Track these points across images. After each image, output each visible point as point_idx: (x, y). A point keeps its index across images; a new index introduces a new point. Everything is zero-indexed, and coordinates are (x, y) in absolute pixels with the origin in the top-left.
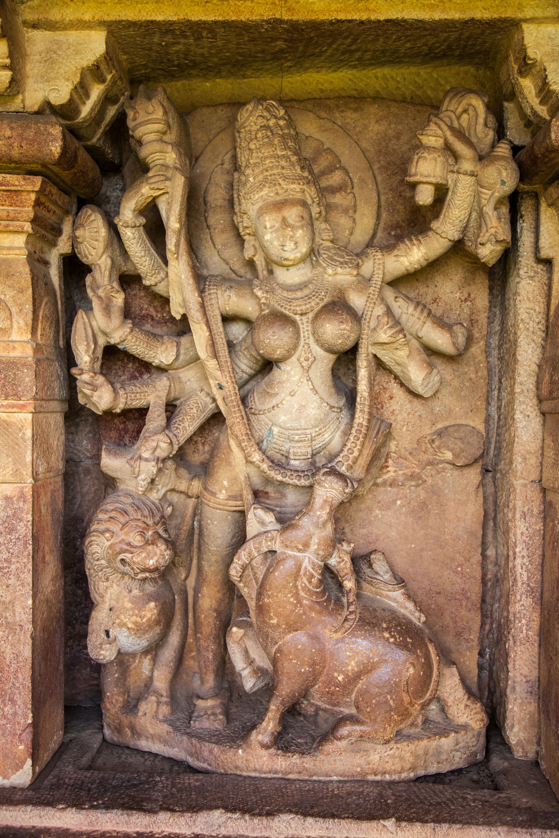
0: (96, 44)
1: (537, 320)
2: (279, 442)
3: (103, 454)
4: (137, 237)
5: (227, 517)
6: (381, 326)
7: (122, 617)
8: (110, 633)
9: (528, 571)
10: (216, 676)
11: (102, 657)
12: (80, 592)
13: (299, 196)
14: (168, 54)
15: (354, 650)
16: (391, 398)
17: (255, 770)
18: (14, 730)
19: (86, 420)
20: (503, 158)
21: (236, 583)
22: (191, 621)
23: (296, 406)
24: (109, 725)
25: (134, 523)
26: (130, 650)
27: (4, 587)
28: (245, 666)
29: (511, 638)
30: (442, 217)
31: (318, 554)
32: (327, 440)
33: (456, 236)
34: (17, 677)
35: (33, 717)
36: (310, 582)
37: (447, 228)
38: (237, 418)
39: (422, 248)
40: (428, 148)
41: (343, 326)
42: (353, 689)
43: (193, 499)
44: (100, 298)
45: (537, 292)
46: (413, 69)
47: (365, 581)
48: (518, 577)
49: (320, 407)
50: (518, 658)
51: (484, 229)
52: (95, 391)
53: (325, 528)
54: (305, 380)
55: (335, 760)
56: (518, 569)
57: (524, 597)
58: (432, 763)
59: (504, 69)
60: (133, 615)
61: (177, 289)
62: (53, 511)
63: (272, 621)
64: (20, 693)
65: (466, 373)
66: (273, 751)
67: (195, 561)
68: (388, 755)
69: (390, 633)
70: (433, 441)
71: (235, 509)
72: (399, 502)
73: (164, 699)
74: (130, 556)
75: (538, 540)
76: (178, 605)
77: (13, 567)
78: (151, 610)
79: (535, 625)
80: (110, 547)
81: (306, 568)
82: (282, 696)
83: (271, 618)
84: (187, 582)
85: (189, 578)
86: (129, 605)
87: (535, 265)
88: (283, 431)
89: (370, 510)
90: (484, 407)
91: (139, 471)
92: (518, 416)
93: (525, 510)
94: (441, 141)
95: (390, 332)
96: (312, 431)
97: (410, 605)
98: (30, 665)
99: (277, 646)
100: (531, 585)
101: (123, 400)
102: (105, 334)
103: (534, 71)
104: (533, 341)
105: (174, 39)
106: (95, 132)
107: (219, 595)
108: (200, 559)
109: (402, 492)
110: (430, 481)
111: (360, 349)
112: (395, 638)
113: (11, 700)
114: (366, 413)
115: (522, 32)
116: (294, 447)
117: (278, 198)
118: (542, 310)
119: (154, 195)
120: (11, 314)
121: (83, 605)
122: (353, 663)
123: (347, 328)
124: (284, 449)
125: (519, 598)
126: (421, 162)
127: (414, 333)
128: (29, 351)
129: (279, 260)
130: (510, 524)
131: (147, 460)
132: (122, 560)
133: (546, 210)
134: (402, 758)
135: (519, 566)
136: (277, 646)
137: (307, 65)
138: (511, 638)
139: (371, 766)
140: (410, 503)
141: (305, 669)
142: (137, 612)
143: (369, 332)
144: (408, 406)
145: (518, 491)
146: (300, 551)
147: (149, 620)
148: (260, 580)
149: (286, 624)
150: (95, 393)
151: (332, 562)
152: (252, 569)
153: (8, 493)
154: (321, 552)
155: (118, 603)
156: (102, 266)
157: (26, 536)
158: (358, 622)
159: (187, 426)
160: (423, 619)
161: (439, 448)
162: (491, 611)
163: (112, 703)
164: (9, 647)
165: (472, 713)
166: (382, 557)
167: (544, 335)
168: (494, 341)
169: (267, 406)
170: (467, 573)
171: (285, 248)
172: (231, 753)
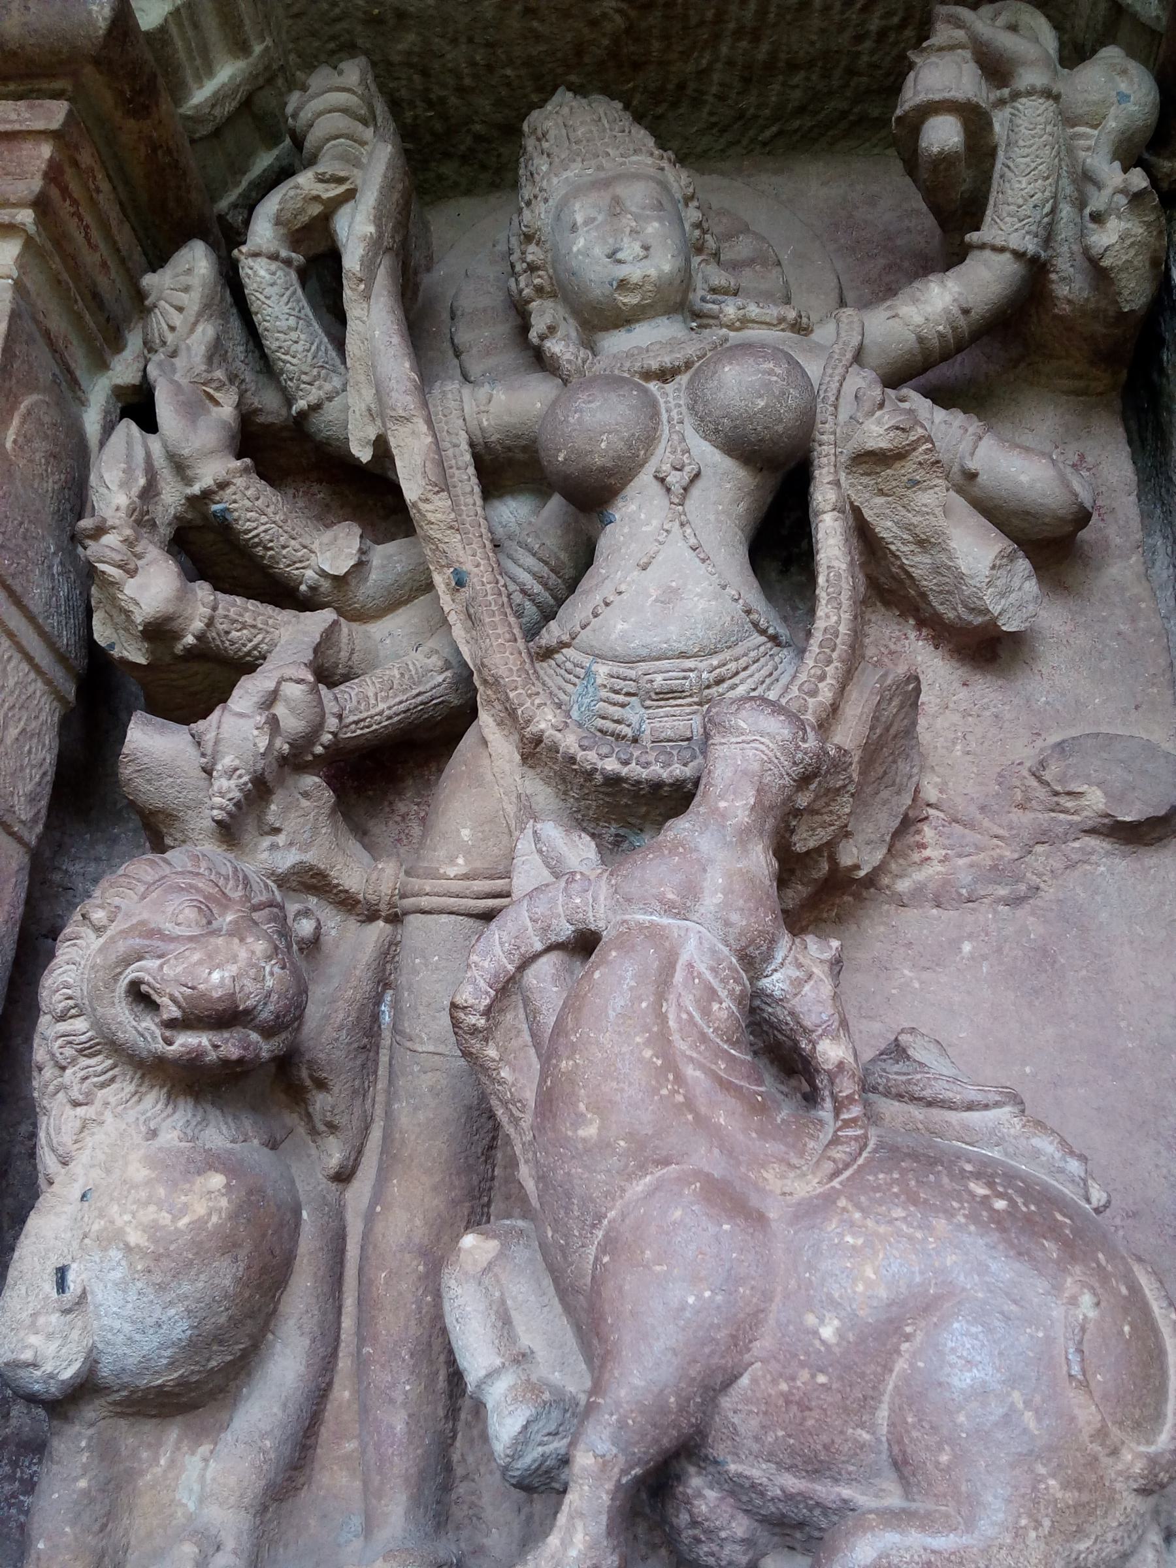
8: (71, 1276)
10: (416, 1501)
15: (866, 1261)
22: (348, 1323)
23: (654, 593)
25: (181, 881)
26: (132, 1362)
28: (498, 1362)
31: (727, 924)
33: (1030, 246)
36: (706, 1013)
37: (1009, 224)
38: (498, 636)
52: (132, 573)
53: (745, 851)
60: (147, 1203)
61: (362, 378)
63: (581, 1133)
65: (1105, 620)
67: (376, 1134)
69: (991, 1185)
70: (1043, 764)
72: (967, 947)
74: (151, 964)
76: (309, 1243)
78: (208, 1199)
81: (690, 966)
84: (348, 1195)
85: (356, 1184)
89: (884, 967)
91: (216, 743)
96: (703, 665)
97: (1047, 1146)
99: (600, 1234)
106: (225, 188)
109: (970, 918)
110: (1050, 892)
111: (817, 473)
114: (844, 607)
117: (602, 175)
119: (325, 196)
123: (778, 371)
127: (956, 469)
129: (607, 290)
131: (241, 715)
140: (999, 950)
141: (699, 1297)
142: (162, 1192)
144: (963, 693)
146: (670, 909)
147: (199, 1224)
151: (776, 982)
154: (735, 917)
155: (108, 1171)
156: (195, 347)
158: (875, 1151)
159: (371, 694)
171: (619, 256)
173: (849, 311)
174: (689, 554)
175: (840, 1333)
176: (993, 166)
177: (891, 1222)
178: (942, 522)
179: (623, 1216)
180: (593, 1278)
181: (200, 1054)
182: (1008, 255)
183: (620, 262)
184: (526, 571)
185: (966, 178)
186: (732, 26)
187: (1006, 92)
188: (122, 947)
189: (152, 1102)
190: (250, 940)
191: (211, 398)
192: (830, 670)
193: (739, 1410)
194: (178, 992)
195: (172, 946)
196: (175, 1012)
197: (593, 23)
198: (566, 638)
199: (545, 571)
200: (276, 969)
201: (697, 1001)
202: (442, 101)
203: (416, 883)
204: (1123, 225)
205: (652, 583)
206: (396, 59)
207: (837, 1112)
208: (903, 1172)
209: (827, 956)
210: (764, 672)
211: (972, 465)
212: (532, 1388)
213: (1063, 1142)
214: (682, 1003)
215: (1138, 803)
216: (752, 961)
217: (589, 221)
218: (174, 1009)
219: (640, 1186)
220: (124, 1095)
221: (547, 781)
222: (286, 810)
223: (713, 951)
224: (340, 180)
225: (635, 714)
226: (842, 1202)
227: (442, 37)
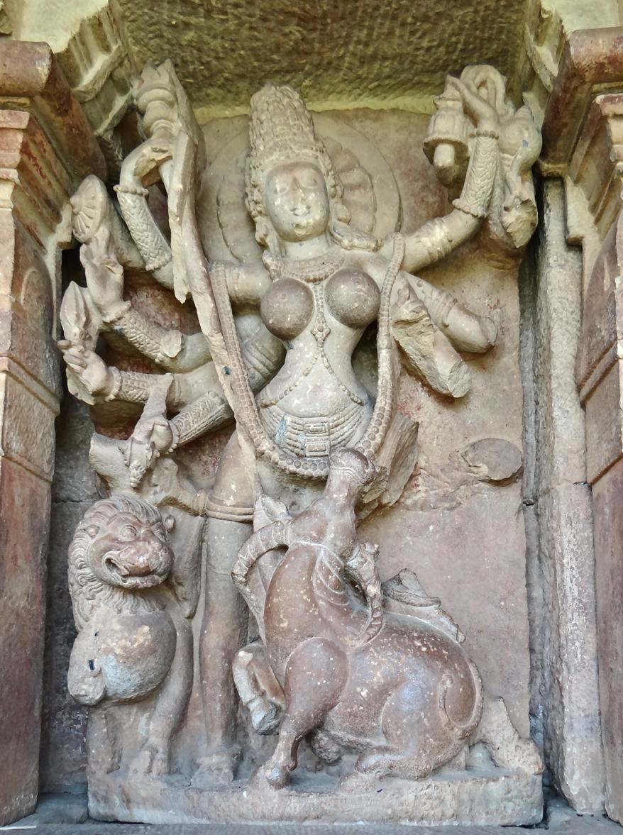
1: (570, 310)
3: (92, 442)
9: (578, 584)
17: (264, 817)
21: (242, 587)
23: (311, 387)
25: (123, 517)
29: (564, 667)
31: (335, 545)
32: (346, 434)
36: (327, 579)
39: (444, 227)
42: (380, 708)
45: (568, 280)
47: (393, 598)
49: (336, 390)
50: (573, 688)
56: (568, 583)
57: (576, 614)
58: (480, 813)
59: (522, 57)
61: (180, 263)
63: (282, 625)
66: (284, 791)
68: (425, 794)
69: (422, 642)
74: (116, 553)
75: (586, 547)
79: (591, 648)
80: (94, 545)
83: (281, 621)
87: (565, 253)
91: (131, 455)
93: (571, 515)
97: (445, 620)
99: (288, 659)
100: (583, 600)
101: (117, 384)
102: (100, 309)
104: (568, 331)
111: (380, 329)
112: (428, 648)
114: (388, 397)
116: (309, 441)
118: (575, 299)
122: (379, 674)
124: (299, 445)
125: (570, 616)
127: (440, 321)
130: (555, 535)
132: (109, 561)
133: (573, 190)
134: (442, 801)
135: (568, 579)
136: (288, 659)
138: (564, 667)
141: (322, 682)
143: (390, 308)
145: (561, 494)
148: (269, 583)
150: (85, 371)
151: (353, 563)
152: (260, 570)
160: (461, 638)
165: (524, 755)
167: (579, 325)
168: (529, 350)
169: (280, 392)
170: (512, 608)
172: (234, 799)
173: (399, 236)
174: (325, 370)
178: (431, 349)
179: (296, 654)
183: (296, 215)
186: (355, 39)
188: (102, 545)
190: (152, 542)
192: (381, 428)
193: (335, 717)
194: (128, 565)
195: (123, 546)
196: (126, 572)
197: (285, 35)
198: (273, 402)
200: (163, 553)
201: (323, 575)
205: (308, 383)
209: (374, 550)
210: (356, 420)
211: (446, 322)
214: (318, 577)
215: (500, 472)
218: (126, 571)
225: (302, 438)
226: (371, 649)
227: (209, 35)
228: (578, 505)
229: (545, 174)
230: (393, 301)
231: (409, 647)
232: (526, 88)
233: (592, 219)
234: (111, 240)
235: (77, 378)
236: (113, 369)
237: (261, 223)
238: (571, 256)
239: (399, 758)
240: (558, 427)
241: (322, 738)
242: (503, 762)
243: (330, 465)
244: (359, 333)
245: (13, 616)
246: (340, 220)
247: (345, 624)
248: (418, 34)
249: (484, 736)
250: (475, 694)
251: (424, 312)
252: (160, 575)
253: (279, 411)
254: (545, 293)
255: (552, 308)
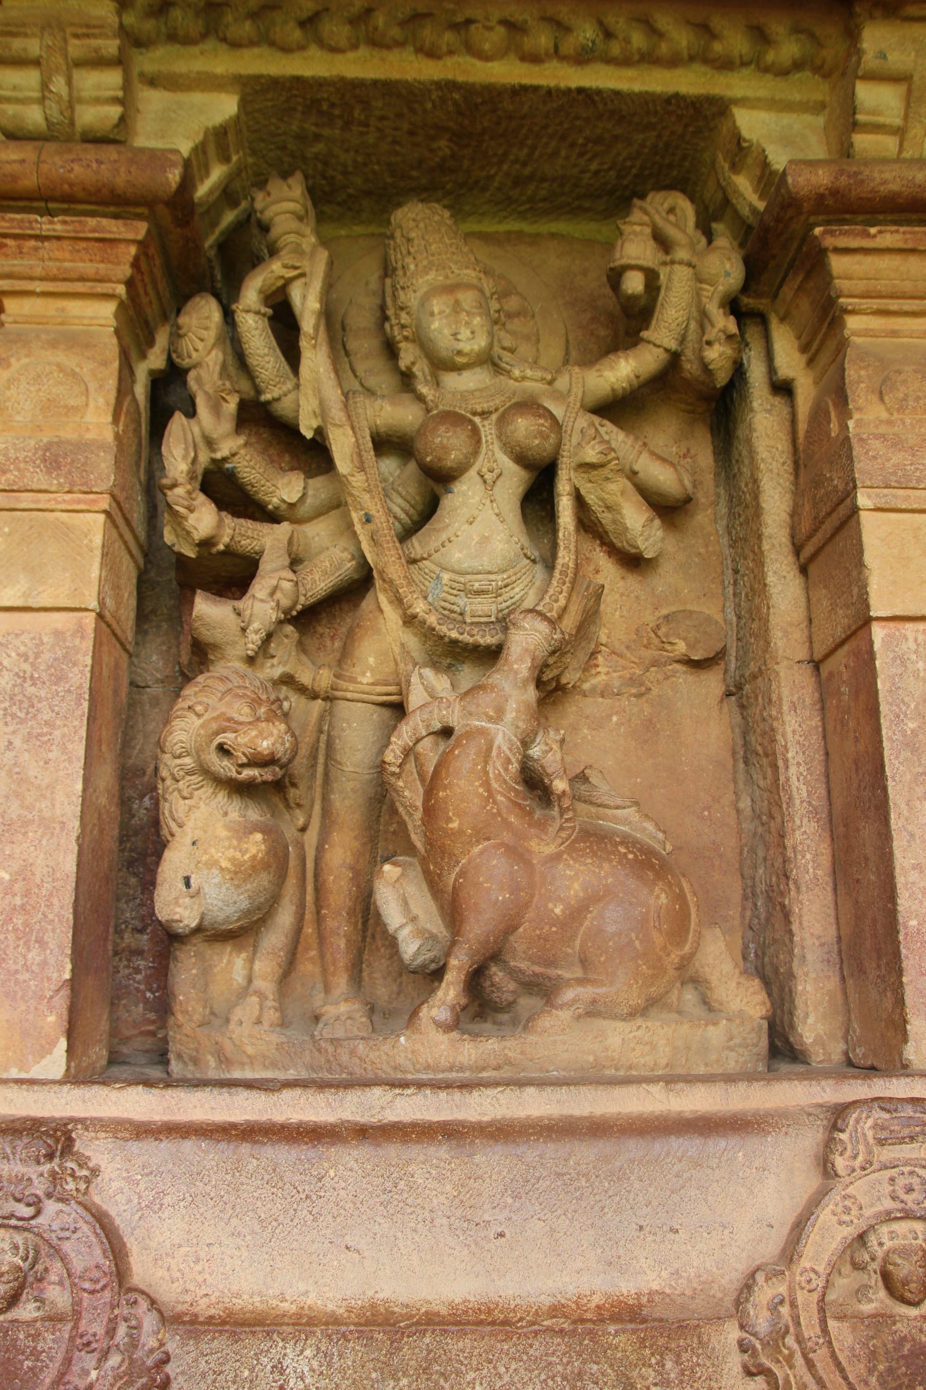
0: (226, 107)
2: (450, 598)
4: (260, 327)
5: (372, 715)
6: (587, 438)
7: (213, 850)
8: (192, 881)
11: (177, 917)
12: (133, 881)
13: (475, 282)
14: (304, 159)
16: (597, 572)
17: (428, 1067)
18: (41, 990)
19: (159, 627)
20: (723, 248)
21: (393, 780)
24: (179, 1056)
25: (240, 692)
26: (221, 916)
27: (42, 763)
29: (792, 886)
30: (654, 322)
31: (517, 727)
32: (517, 597)
33: (673, 345)
34: (52, 904)
35: (73, 970)
36: (506, 770)
37: (664, 332)
40: (635, 233)
41: (541, 421)
43: (320, 701)
44: (206, 393)
46: (593, 226)
48: (795, 793)
50: (805, 911)
51: (708, 327)
52: (192, 511)
54: (488, 502)
55: (555, 1042)
57: (805, 820)
59: (711, 184)
60: (229, 848)
61: (310, 392)
62: (116, 692)
63: (451, 825)
64: (54, 930)
66: (455, 1035)
69: (627, 848)
70: (658, 627)
71: (385, 698)
72: (615, 718)
73: (270, 1003)
75: (815, 739)
76: (293, 862)
77: (57, 733)
78: (256, 845)
79: (825, 860)
80: (202, 726)
81: (499, 747)
82: (469, 940)
83: (449, 820)
85: (308, 832)
86: (223, 833)
88: (457, 578)
89: (575, 728)
90: (720, 591)
91: (251, 615)
92: (771, 579)
93: (795, 699)
94: (648, 230)
95: (598, 448)
97: (650, 826)
98: (74, 884)
99: (457, 869)
101: (230, 531)
103: (749, 161)
105: (316, 125)
107: (356, 844)
108: (325, 799)
109: (617, 704)
110: (655, 691)
113: (40, 942)
115: (733, 116)
117: (448, 282)
119: (287, 276)
120: (87, 390)
121: (138, 901)
122: (576, 886)
125: (798, 822)
126: (627, 245)
127: (627, 467)
128: (109, 435)
129: (450, 354)
130: (775, 724)
131: (262, 601)
135: (795, 778)
137: (467, 208)
139: (609, 1053)
142: (235, 843)
144: (621, 584)
145: (782, 674)
146: (490, 719)
147: (254, 857)
149: (473, 828)
151: (535, 751)
152: (416, 759)
153: (59, 626)
154: (521, 724)
155: (205, 832)
156: (211, 364)
157: (80, 687)
160: (669, 847)
161: (667, 636)
162: (753, 886)
163: (187, 1012)
164: (42, 856)
166: (600, 776)
167: (792, 478)
169: (433, 544)
171: (459, 337)
172: (386, 1047)
174: (494, 518)
175: (563, 911)
176: (658, 295)
177: (586, 865)
178: (621, 500)
179: (469, 862)
180: (454, 888)
181: (255, 778)
182: (661, 350)
184: (399, 507)
185: (643, 302)
186: (512, 157)
187: (668, 258)
188: (214, 726)
189: (221, 796)
191: (224, 399)
192: (565, 588)
193: (518, 942)
194: (248, 751)
196: (245, 760)
197: (432, 151)
198: (425, 556)
199: (407, 507)
202: (333, 178)
203: (342, 684)
204: (722, 349)
206: (309, 155)
207: (561, 816)
208: (591, 843)
209: (558, 738)
211: (636, 468)
212: (420, 932)
213: (657, 824)
214: (495, 767)
216: (526, 744)
217: (441, 313)
219: (477, 849)
220: (208, 794)
221: (415, 635)
222: (278, 645)
223: (510, 740)
224: (296, 268)
225: (462, 601)
226: (565, 856)
228: (803, 688)
229: (744, 309)
230: (575, 441)
231: (613, 853)
232: (716, 218)
233: (804, 359)
234: (224, 367)
235: (180, 524)
236: (224, 514)
237: (406, 350)
238: (778, 402)
239: (601, 990)
240: (774, 596)
241: (497, 974)
242: (721, 1004)
243: (506, 629)
244: (536, 474)
245: (96, 815)
246: (504, 349)
247: (530, 825)
248: (587, 157)
249: (697, 972)
250: (690, 915)
251: (613, 455)
252: (281, 768)
253: (433, 567)
254: (749, 441)
255: (759, 457)
